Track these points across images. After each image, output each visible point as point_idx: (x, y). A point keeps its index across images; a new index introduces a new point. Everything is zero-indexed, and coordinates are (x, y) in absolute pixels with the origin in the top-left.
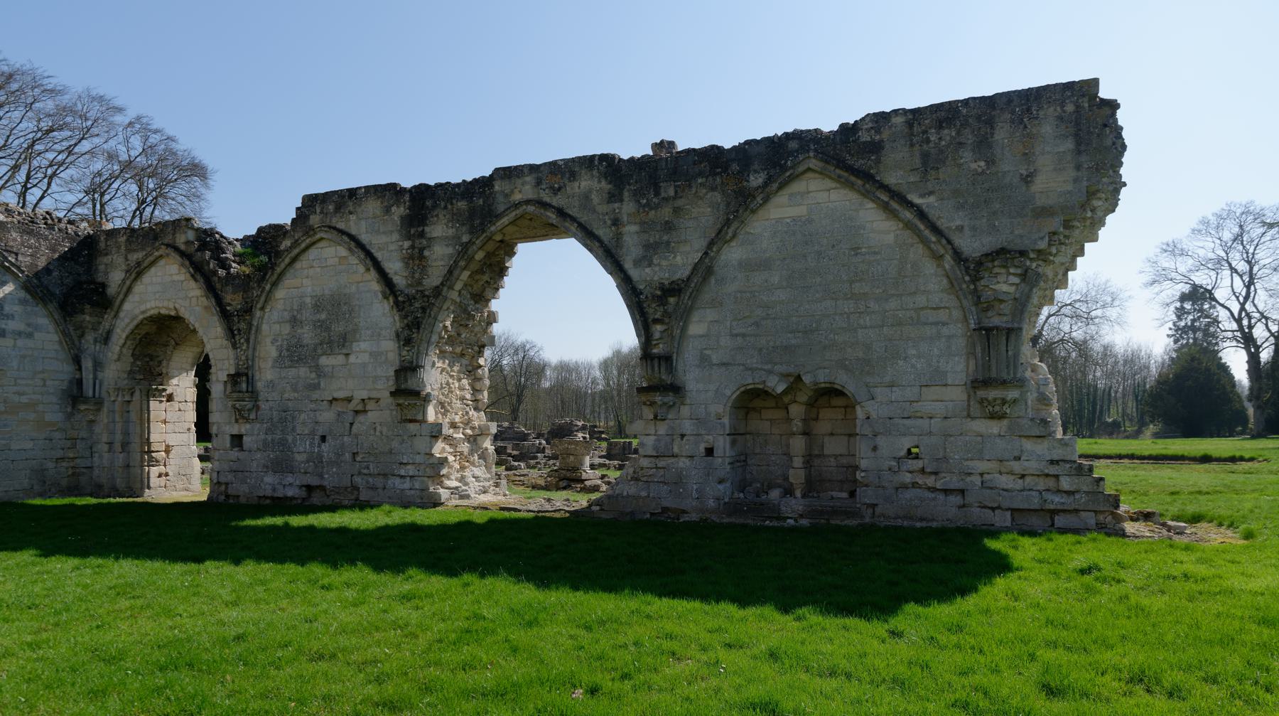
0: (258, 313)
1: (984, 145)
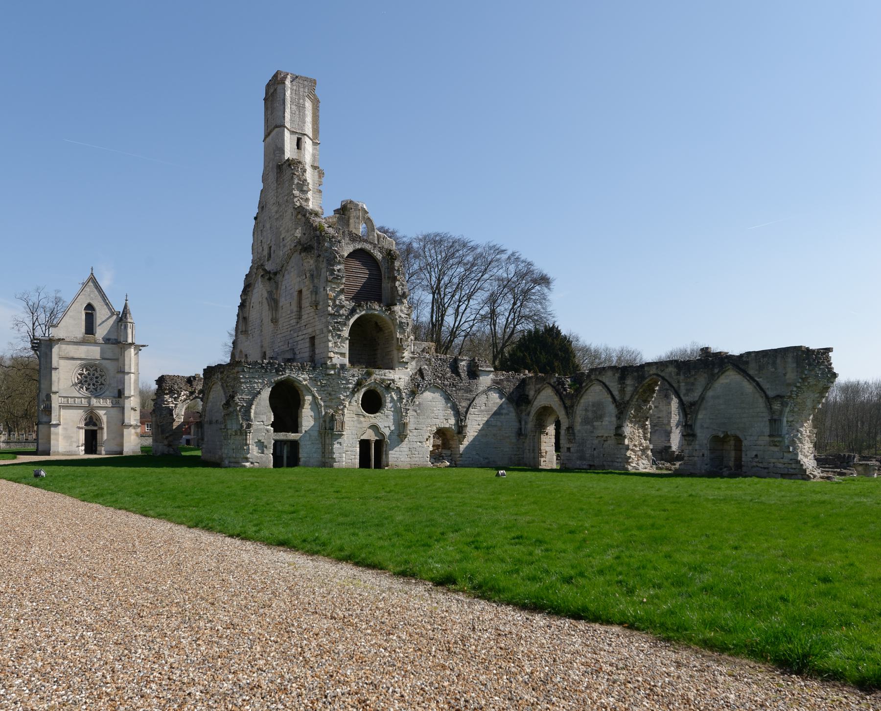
1: (774, 364)
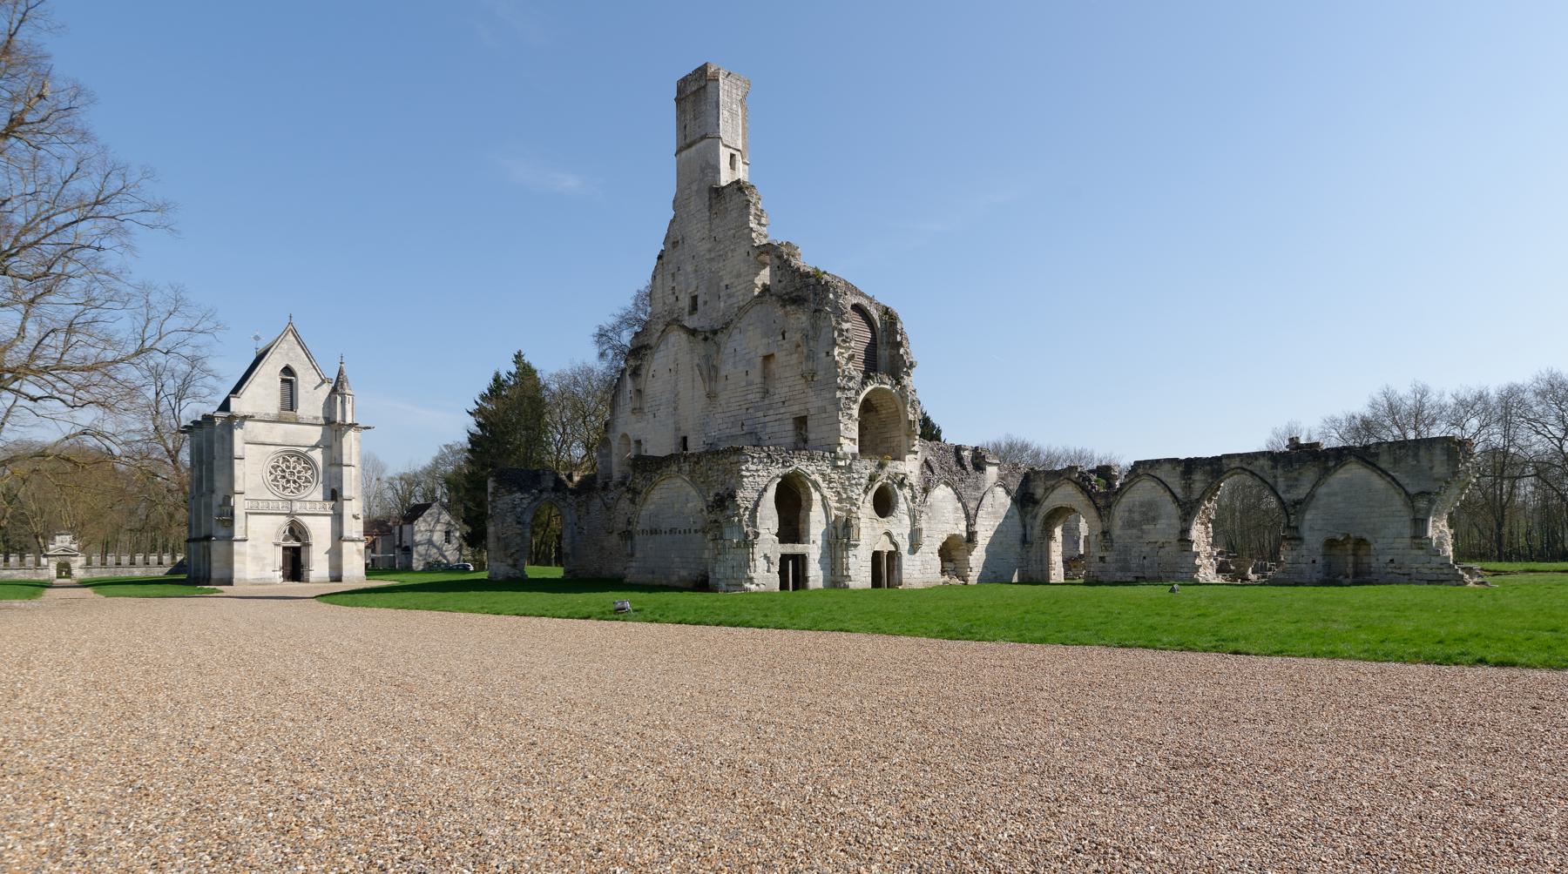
0: (1114, 508)
1: (1416, 456)
